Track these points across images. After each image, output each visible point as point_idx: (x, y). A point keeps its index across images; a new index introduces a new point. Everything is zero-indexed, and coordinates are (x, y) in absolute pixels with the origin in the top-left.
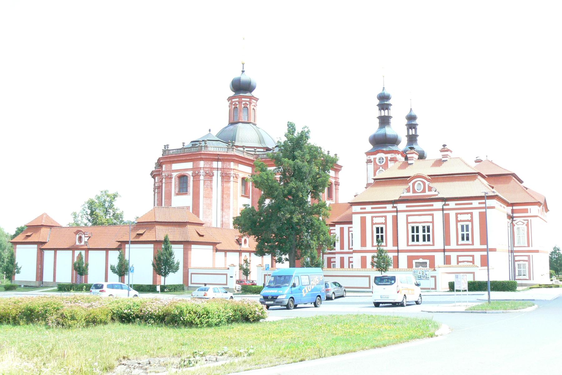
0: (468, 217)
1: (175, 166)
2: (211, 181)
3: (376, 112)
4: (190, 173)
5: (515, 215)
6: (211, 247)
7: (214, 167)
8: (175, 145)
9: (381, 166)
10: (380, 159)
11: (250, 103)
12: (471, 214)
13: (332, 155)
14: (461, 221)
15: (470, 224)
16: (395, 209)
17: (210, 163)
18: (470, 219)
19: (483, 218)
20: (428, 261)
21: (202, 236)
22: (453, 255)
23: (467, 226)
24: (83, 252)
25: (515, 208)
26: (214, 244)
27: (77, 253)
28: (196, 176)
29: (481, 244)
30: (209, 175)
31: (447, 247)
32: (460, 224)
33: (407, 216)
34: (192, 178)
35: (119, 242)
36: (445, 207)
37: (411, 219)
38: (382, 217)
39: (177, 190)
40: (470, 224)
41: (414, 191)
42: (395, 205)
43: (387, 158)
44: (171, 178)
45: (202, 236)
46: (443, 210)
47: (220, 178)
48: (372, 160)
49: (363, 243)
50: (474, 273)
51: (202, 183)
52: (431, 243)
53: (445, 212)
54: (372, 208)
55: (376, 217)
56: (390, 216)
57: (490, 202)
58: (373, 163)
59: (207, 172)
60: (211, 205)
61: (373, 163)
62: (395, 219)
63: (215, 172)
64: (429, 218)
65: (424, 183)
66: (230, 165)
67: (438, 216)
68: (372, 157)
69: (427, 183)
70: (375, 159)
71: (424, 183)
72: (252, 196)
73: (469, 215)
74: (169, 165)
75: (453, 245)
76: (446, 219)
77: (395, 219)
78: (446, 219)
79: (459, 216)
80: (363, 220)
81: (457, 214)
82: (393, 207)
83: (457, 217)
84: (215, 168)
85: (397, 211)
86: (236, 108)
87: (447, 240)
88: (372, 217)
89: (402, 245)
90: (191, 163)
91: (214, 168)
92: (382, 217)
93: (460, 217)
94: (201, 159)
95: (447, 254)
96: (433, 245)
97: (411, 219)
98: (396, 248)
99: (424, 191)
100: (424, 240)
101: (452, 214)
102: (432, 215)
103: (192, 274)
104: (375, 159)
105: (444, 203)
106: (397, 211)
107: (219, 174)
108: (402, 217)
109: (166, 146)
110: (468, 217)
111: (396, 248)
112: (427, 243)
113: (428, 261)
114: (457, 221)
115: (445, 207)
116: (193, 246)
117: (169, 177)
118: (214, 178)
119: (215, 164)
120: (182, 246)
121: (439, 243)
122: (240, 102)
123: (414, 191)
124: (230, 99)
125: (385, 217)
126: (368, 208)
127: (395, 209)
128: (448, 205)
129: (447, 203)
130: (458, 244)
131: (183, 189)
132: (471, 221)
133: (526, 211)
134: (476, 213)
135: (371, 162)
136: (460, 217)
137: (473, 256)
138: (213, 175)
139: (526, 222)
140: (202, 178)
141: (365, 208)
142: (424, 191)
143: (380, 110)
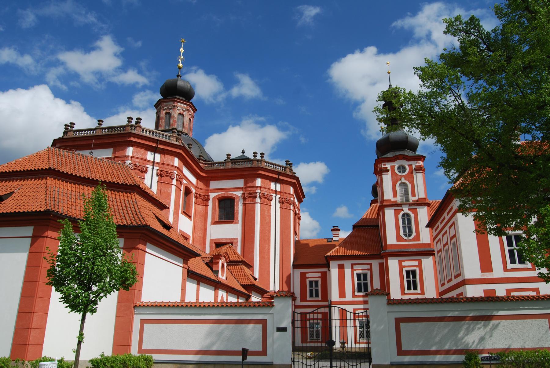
7: (148, 159)
9: (402, 176)
17: (142, 151)
58: (390, 173)
59: (138, 164)
63: (150, 167)
66: (174, 161)
70: (393, 168)
72: (195, 218)
84: (150, 161)
90: (111, 150)
91: (148, 161)
119: (150, 156)
138: (146, 172)
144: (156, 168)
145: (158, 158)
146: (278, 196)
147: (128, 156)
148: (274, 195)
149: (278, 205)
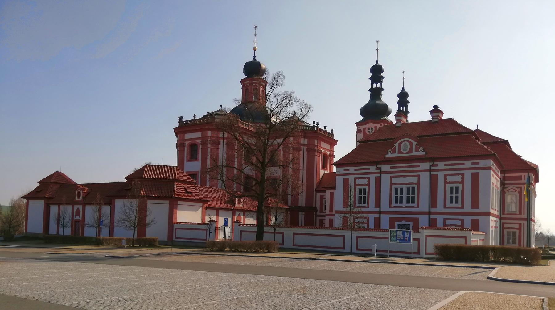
1: (188, 136)
2: (218, 149)
4: (199, 142)
5: (506, 182)
8: (188, 117)
10: (369, 129)
14: (450, 182)
16: (379, 171)
18: (460, 180)
19: (475, 178)
21: (191, 193)
22: (440, 219)
23: (457, 188)
24: (81, 207)
25: (507, 175)
26: (204, 202)
28: (204, 143)
29: (472, 208)
30: (216, 143)
32: (448, 186)
33: (391, 177)
34: (201, 146)
35: (108, 196)
36: (433, 168)
37: (394, 180)
38: (365, 178)
39: (189, 157)
40: (460, 186)
41: (400, 152)
42: (379, 166)
43: (376, 127)
44: (184, 146)
45: (191, 193)
46: (430, 170)
48: (362, 130)
51: (209, 150)
52: (415, 205)
53: (433, 173)
54: (355, 170)
55: (359, 178)
56: (373, 178)
57: (483, 163)
61: (362, 133)
63: (221, 141)
64: (415, 180)
65: (411, 144)
67: (425, 178)
68: (362, 127)
70: (364, 129)
71: (411, 144)
73: (460, 176)
74: (182, 135)
76: (433, 181)
77: (378, 181)
78: (433, 181)
79: (448, 177)
81: (446, 176)
82: (377, 168)
88: (355, 179)
92: (365, 178)
93: (449, 179)
94: (209, 129)
96: (418, 207)
97: (394, 180)
98: (378, 210)
99: (410, 151)
100: (408, 202)
101: (441, 176)
102: (418, 176)
103: (176, 229)
104: (364, 129)
105: (431, 163)
106: (381, 173)
107: (225, 143)
108: (385, 179)
110: (459, 178)
114: (446, 183)
115: (433, 168)
116: (179, 202)
118: (221, 147)
119: (221, 134)
120: (168, 202)
121: (424, 206)
123: (400, 152)
126: (352, 170)
127: (379, 171)
128: (437, 165)
129: (435, 163)
130: (445, 207)
134: (468, 175)
135: (361, 132)
136: (449, 179)
137: (462, 220)
138: (219, 144)
139: (518, 190)
140: (209, 146)
141: (348, 170)
142: (410, 151)
144: (225, 141)
146: (306, 147)
147: (208, 137)
148: (302, 147)
149: (306, 153)
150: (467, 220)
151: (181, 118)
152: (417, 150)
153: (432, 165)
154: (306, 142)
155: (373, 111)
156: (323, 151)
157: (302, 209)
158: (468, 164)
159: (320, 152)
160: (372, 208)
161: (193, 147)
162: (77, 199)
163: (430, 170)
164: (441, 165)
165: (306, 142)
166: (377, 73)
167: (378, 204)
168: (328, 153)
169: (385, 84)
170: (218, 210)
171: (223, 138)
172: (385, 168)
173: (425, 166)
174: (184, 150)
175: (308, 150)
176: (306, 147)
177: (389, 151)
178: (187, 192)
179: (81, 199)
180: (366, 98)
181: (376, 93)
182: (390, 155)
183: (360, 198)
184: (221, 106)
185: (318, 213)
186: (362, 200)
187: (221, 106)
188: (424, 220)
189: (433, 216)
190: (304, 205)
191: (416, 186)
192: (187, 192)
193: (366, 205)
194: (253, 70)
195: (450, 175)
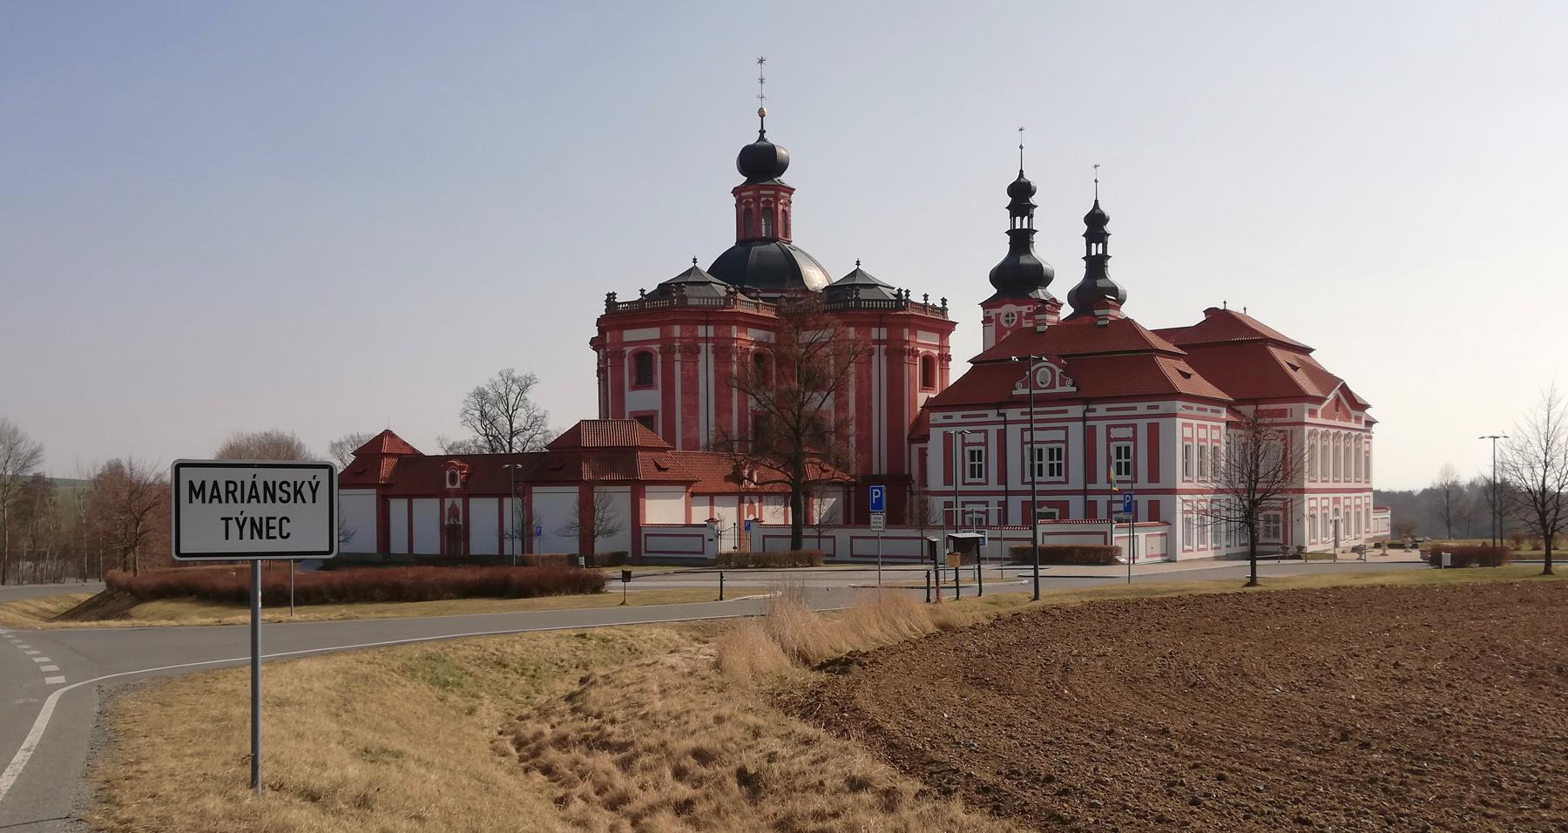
0: (1128, 432)
1: (630, 335)
2: (696, 363)
3: (1004, 221)
4: (656, 347)
6: (683, 488)
8: (628, 294)
11: (777, 199)
12: (1134, 426)
13: (935, 301)
15: (1131, 444)
19: (1153, 431)
20: (1057, 511)
22: (1102, 501)
23: (1127, 449)
24: (459, 502)
25: (1263, 407)
26: (688, 483)
27: (448, 502)
28: (667, 352)
30: (691, 351)
31: (1090, 487)
32: (1113, 445)
43: (1020, 313)
46: (1084, 419)
47: (711, 357)
49: (948, 479)
50: (1105, 534)
51: (678, 366)
56: (993, 431)
57: (1164, 406)
60: (696, 407)
62: (1002, 435)
63: (703, 346)
64: (1060, 435)
67: (1076, 430)
68: (993, 312)
69: (1058, 371)
70: (998, 315)
75: (1101, 483)
76: (1090, 434)
77: (1002, 435)
78: (1090, 434)
80: (948, 439)
81: (1109, 427)
83: (1108, 433)
85: (1005, 422)
86: (748, 210)
87: (1090, 475)
89: (1014, 483)
93: (1115, 433)
94: (675, 322)
95: (1090, 498)
96: (1067, 482)
98: (1002, 488)
99: (1052, 385)
100: (1052, 474)
101: (1101, 427)
102: (1066, 428)
104: (998, 315)
106: (1005, 422)
108: (1013, 433)
109: (611, 297)
110: (1128, 432)
111: (1002, 488)
112: (1056, 478)
113: (1057, 511)
114: (1109, 440)
116: (648, 488)
117: (621, 355)
118: (702, 357)
119: (701, 331)
120: (628, 488)
121: (1076, 481)
122: (756, 199)
124: (736, 191)
125: (986, 432)
126: (957, 416)
131: (643, 380)
132: (1134, 439)
133: (1283, 413)
134: (1142, 425)
136: (1115, 433)
138: (699, 351)
140: (678, 356)
142: (1052, 385)
143: (1013, 216)
145: (711, 331)
146: (883, 347)
150: (1143, 502)
151: (611, 297)
152: (1062, 384)
153: (1088, 410)
154: (884, 336)
155: (1018, 277)
156: (921, 350)
157: (878, 480)
158: (1142, 407)
159: (915, 353)
160: (993, 485)
161: (643, 360)
162: (448, 486)
163: (1084, 419)
164: (1101, 410)
165: (884, 336)
166: (1021, 196)
167: (1003, 478)
168: (936, 352)
169: (1040, 220)
170: (712, 497)
171: (707, 339)
172: (1013, 414)
173: (1076, 411)
174: (623, 366)
175: (887, 353)
176: (883, 347)
177: (1018, 384)
178: (660, 469)
179: (458, 485)
180: (1000, 250)
181: (1021, 240)
182: (1020, 391)
183: (973, 467)
184: (695, 261)
185: (915, 488)
186: (976, 471)
187: (695, 261)
188: (1076, 504)
189: (1090, 498)
190: (884, 471)
191: (1063, 446)
192: (660, 469)
193: (983, 480)
194: (761, 164)
195: (1116, 426)
